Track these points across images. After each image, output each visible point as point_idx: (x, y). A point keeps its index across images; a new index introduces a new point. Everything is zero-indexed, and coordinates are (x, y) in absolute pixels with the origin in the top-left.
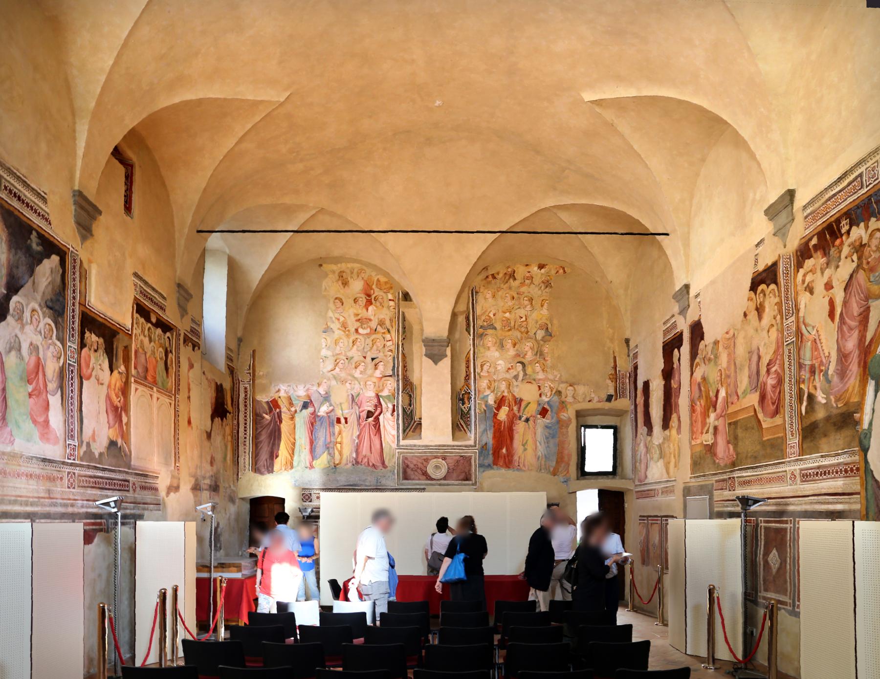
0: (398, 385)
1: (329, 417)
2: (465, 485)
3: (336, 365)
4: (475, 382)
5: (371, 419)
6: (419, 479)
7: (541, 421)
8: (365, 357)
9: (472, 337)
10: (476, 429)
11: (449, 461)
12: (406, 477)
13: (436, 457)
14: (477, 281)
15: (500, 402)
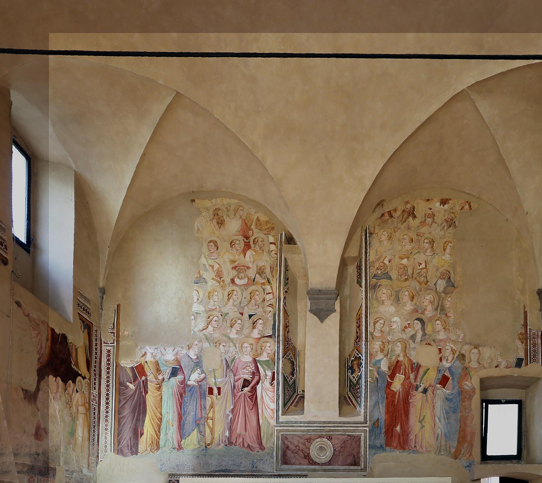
0: (279, 347)
1: (200, 386)
2: (352, 470)
3: (209, 324)
4: (366, 345)
5: (246, 389)
7: (442, 392)
8: (242, 314)
9: (363, 289)
10: (366, 401)
11: (334, 441)
12: (285, 461)
13: (320, 437)
14: (371, 220)
15: (395, 368)
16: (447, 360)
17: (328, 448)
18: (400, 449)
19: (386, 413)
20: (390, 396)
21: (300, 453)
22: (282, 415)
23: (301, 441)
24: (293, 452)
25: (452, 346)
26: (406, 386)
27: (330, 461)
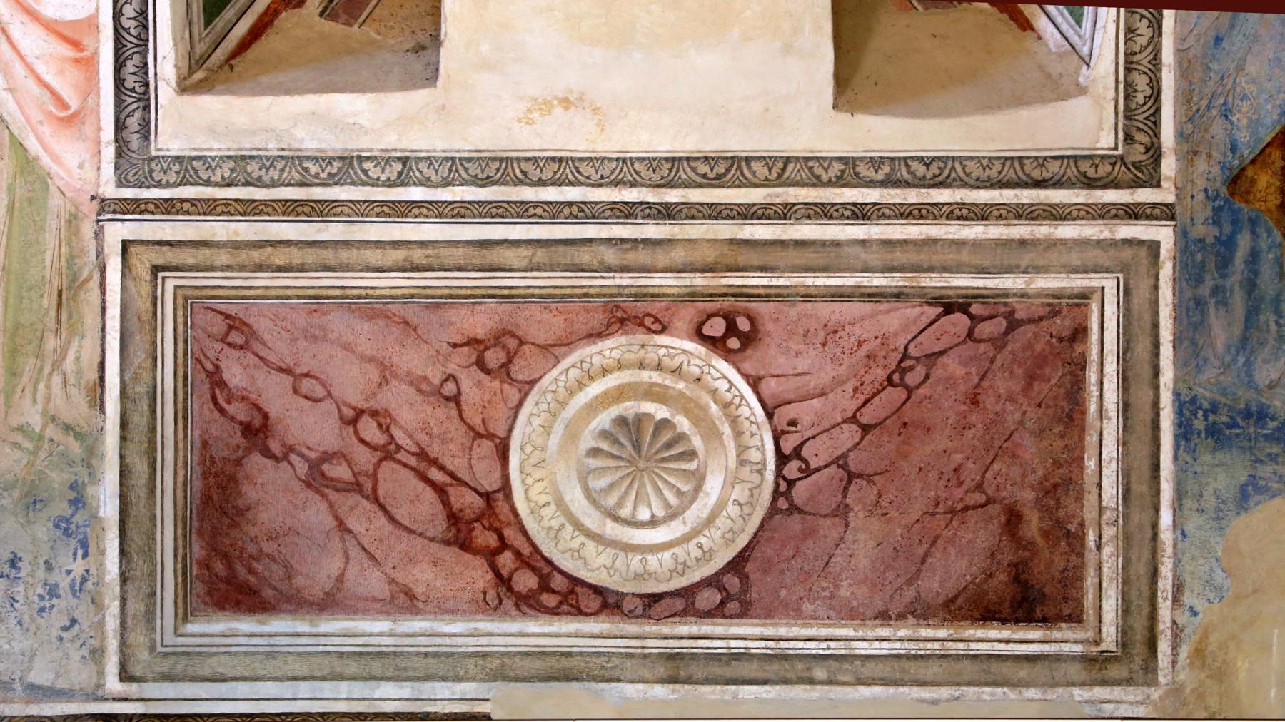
6: (406, 600)
11: (790, 357)
12: (232, 577)
13: (624, 316)
17: (711, 434)
21: (400, 485)
22: (186, 86)
23: (413, 360)
24: (317, 480)
27: (737, 565)
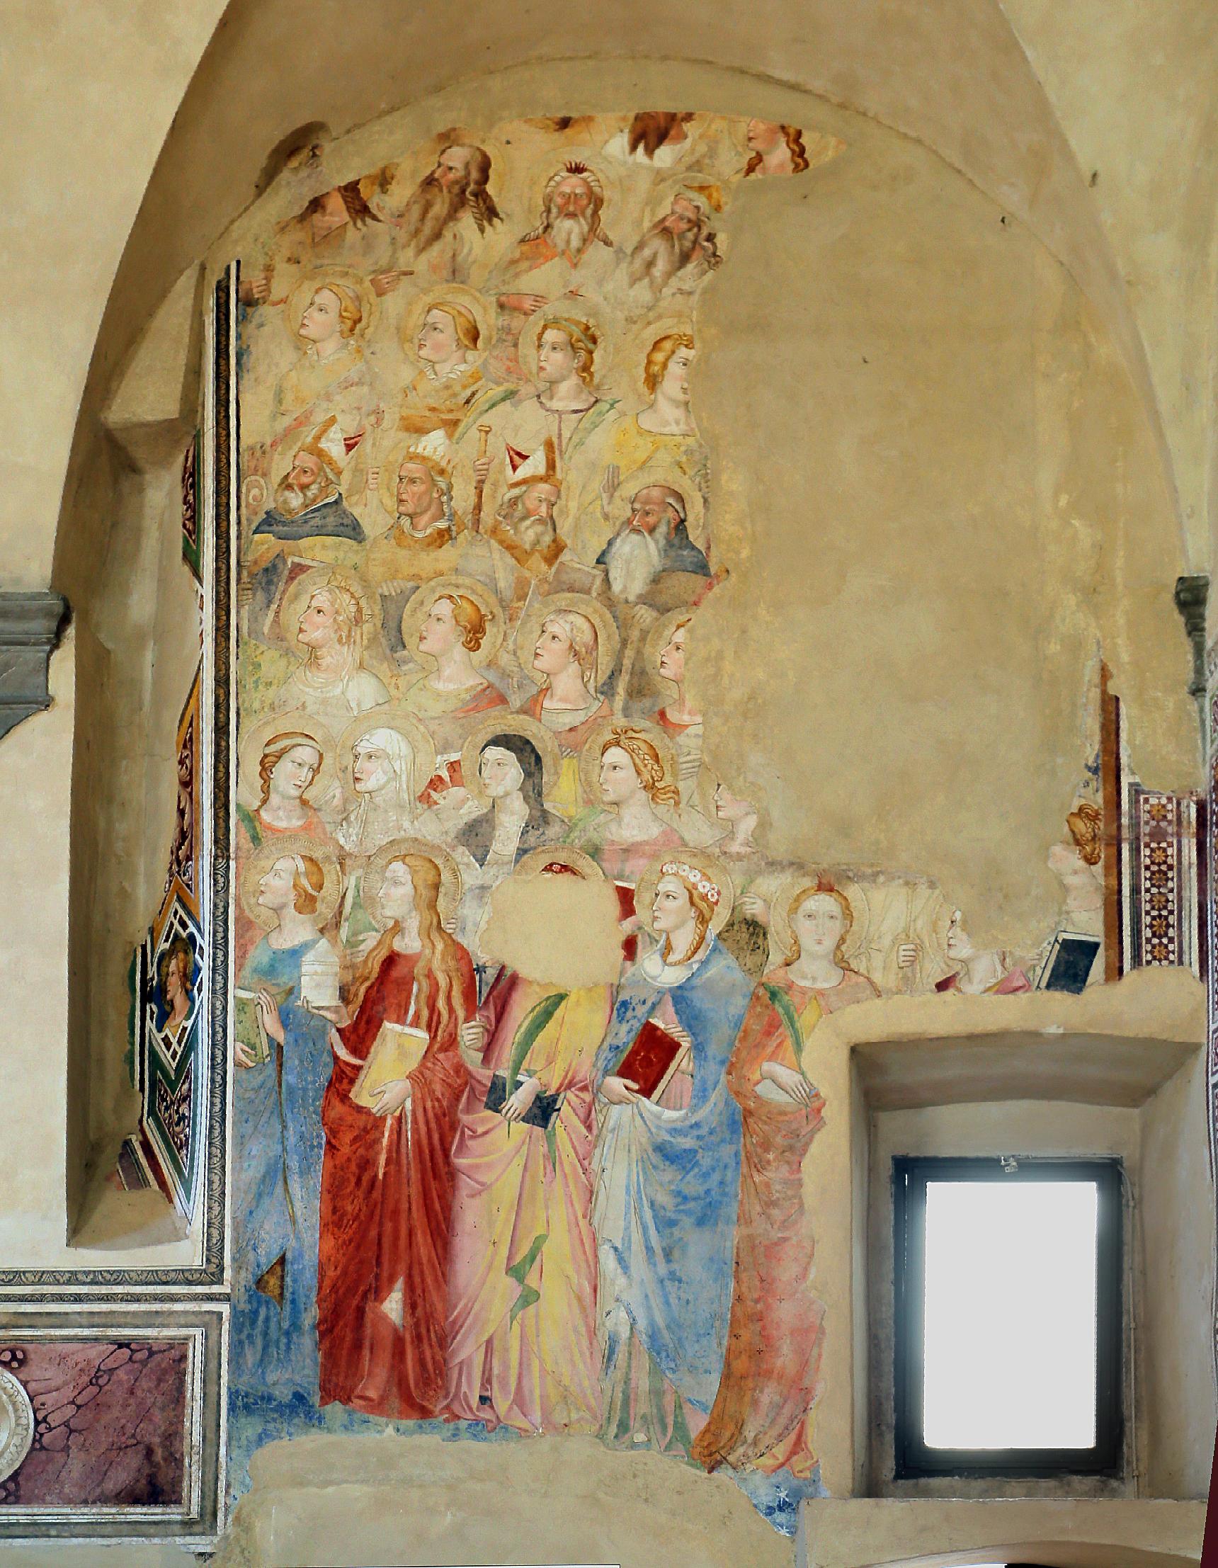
7: (631, 1117)
10: (216, 1166)
15: (378, 994)
16: (668, 948)
18: (402, 1414)
19: (325, 1226)
20: (347, 1137)
25: (694, 877)
26: (438, 1088)
